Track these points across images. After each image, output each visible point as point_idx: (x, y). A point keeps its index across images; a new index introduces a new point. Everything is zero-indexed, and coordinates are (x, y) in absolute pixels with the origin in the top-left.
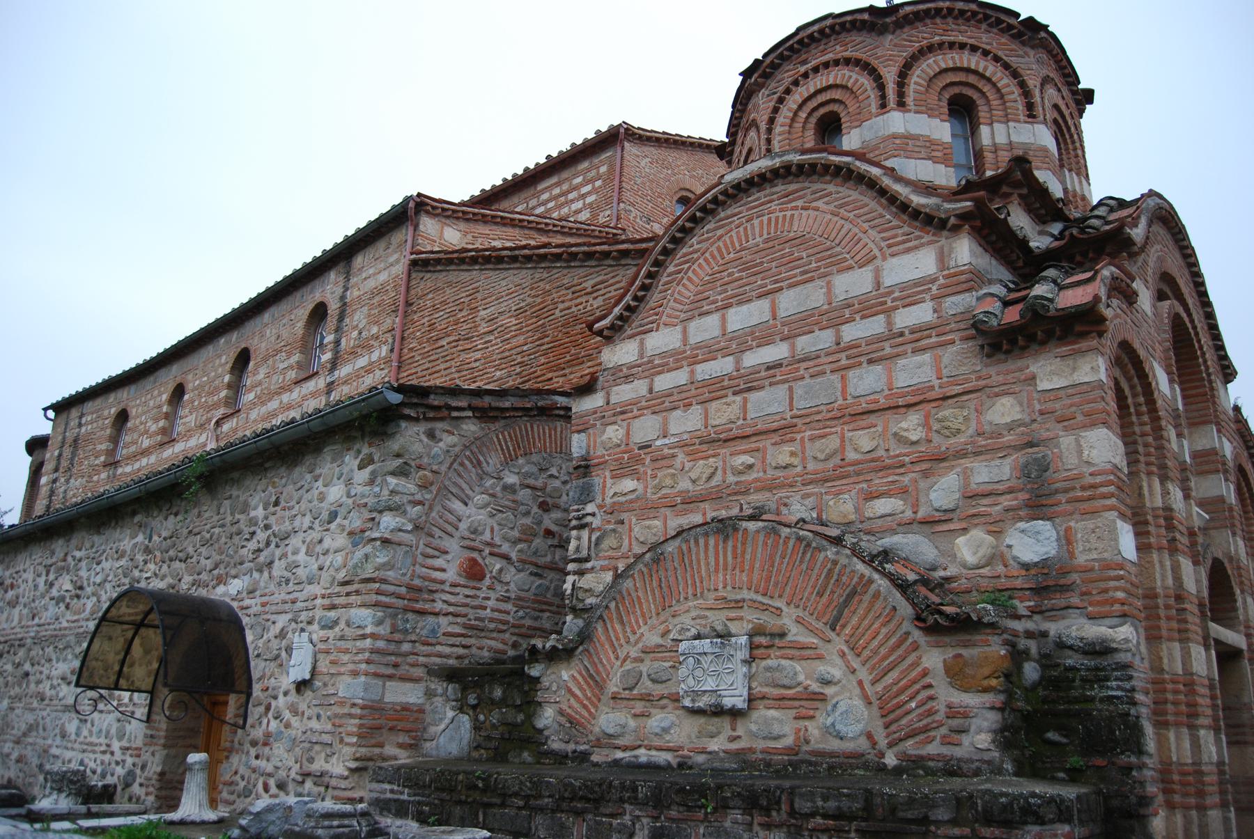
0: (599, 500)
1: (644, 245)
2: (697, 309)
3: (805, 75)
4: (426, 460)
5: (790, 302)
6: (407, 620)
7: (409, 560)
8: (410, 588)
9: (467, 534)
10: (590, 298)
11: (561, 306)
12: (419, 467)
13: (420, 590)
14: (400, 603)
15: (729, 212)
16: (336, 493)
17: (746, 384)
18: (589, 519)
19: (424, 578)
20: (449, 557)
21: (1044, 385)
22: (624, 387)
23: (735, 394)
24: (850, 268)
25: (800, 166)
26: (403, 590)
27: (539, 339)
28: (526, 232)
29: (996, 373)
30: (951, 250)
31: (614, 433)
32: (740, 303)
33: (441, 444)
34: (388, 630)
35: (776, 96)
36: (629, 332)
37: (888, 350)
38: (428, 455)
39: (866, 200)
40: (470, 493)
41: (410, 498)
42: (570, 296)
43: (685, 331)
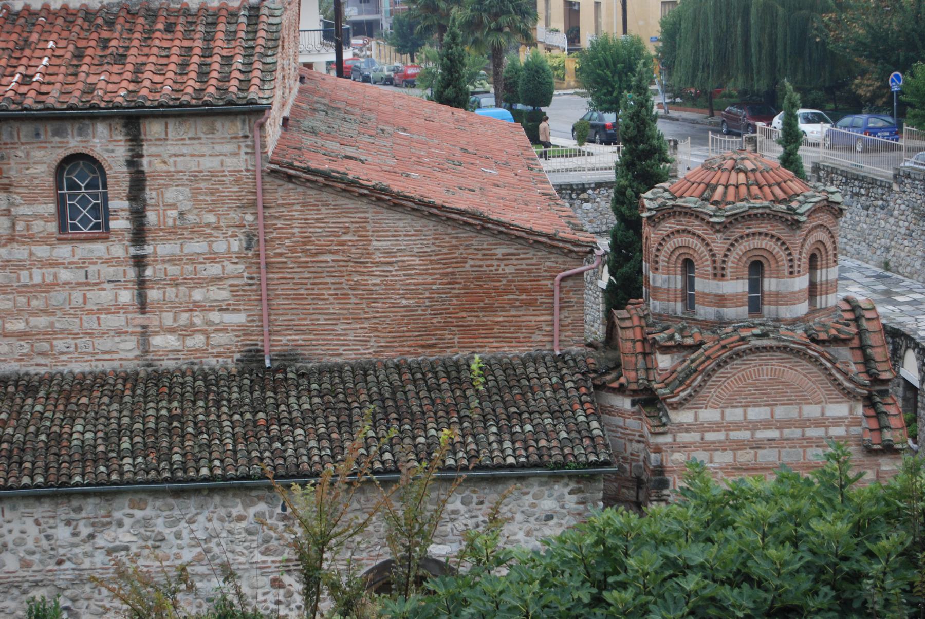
0: (671, 487)
1: (561, 244)
2: (731, 403)
3: (748, 235)
5: (781, 412)
10: (502, 264)
11: (472, 262)
15: (750, 357)
16: (548, 505)
17: (757, 446)
18: (665, 497)
21: (883, 468)
22: (684, 434)
23: (751, 448)
24: (810, 403)
25: (792, 350)
27: (449, 283)
29: (867, 461)
30: (855, 407)
31: (679, 457)
32: (755, 406)
35: (729, 242)
36: (687, 406)
37: (825, 443)
39: (820, 374)
42: (480, 257)
43: (723, 413)
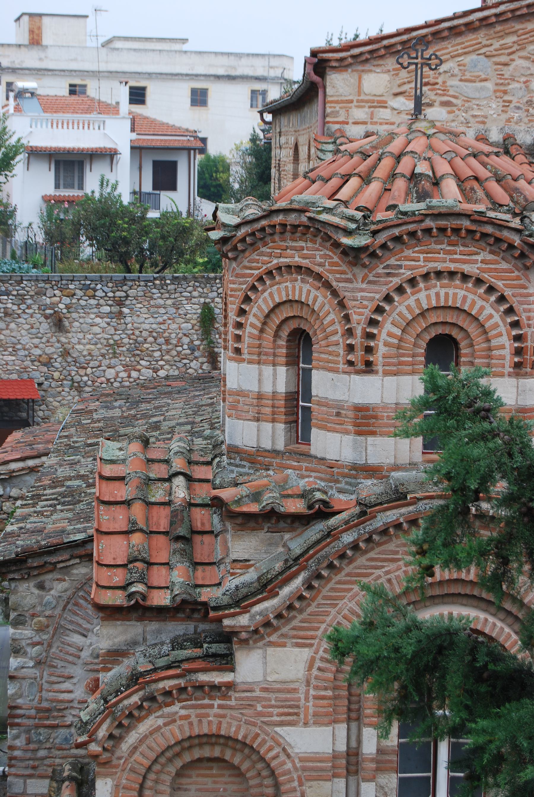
4: (39, 608)
6: (40, 734)
7: (35, 689)
8: (39, 710)
9: (90, 659)
12: (33, 616)
13: (48, 710)
14: (31, 722)
19: (52, 701)
20: (75, 680)
26: (33, 712)
28: (498, 28)
33: (52, 592)
34: (24, 742)
38: (41, 604)
40: (88, 626)
41: (29, 641)
